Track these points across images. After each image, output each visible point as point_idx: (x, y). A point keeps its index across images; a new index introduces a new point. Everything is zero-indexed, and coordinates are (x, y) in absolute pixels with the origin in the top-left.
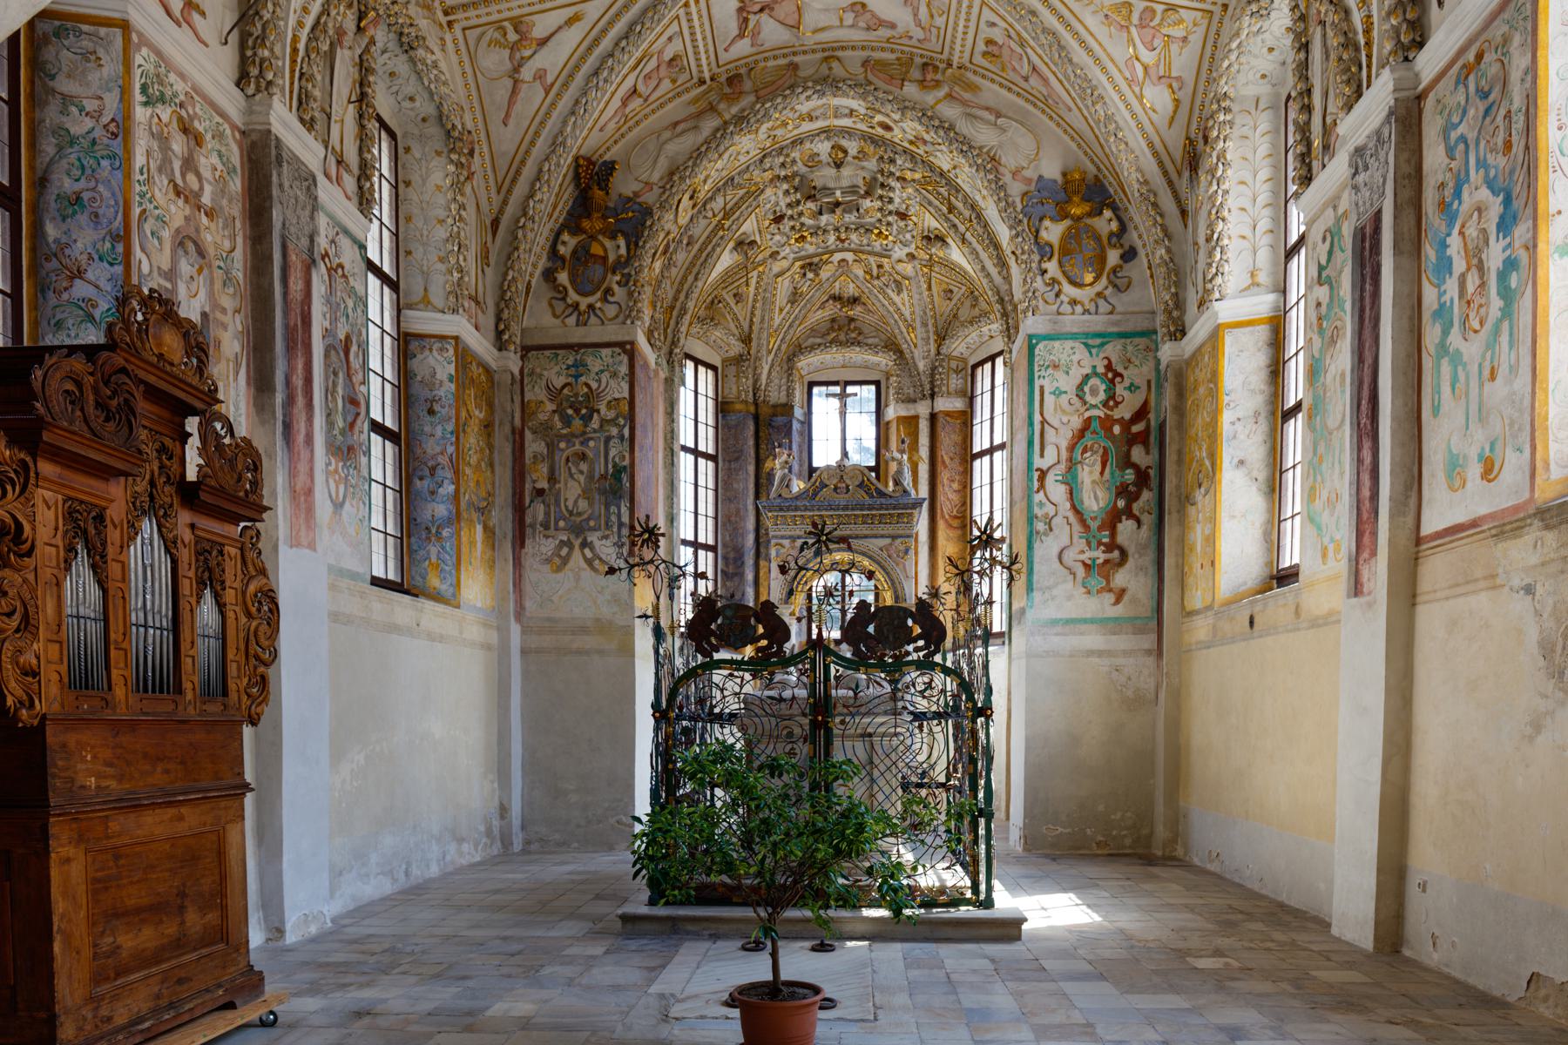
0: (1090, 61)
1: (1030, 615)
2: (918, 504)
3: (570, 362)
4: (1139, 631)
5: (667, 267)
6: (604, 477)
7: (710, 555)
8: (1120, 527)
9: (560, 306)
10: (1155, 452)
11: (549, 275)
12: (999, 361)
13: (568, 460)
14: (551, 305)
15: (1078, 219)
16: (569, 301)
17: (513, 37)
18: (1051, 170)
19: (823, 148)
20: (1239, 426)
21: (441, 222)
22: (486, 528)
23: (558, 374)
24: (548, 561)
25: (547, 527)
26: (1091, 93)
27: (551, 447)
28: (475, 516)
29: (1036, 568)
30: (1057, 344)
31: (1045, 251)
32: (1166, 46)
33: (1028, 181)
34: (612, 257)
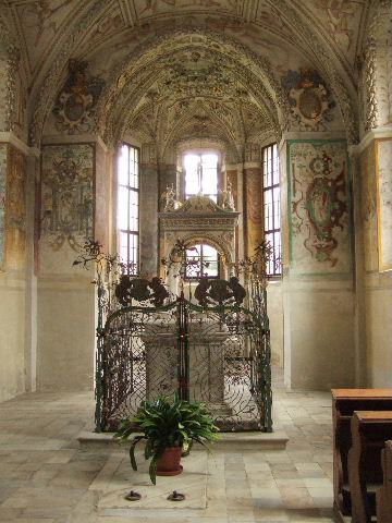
0: (309, 22)
1: (291, 272)
2: (236, 215)
4: (345, 279)
5: (113, 107)
7: (136, 236)
8: (334, 229)
10: (348, 193)
11: (55, 111)
12: (275, 147)
15: (307, 89)
17: (40, 9)
18: (294, 67)
19: (188, 54)
20: (386, 186)
21: (3, 90)
22: (20, 231)
26: (310, 34)
27: (55, 191)
28: (15, 224)
29: (293, 249)
30: (300, 145)
31: (292, 102)
32: (344, 16)
33: (284, 72)
34: (85, 104)
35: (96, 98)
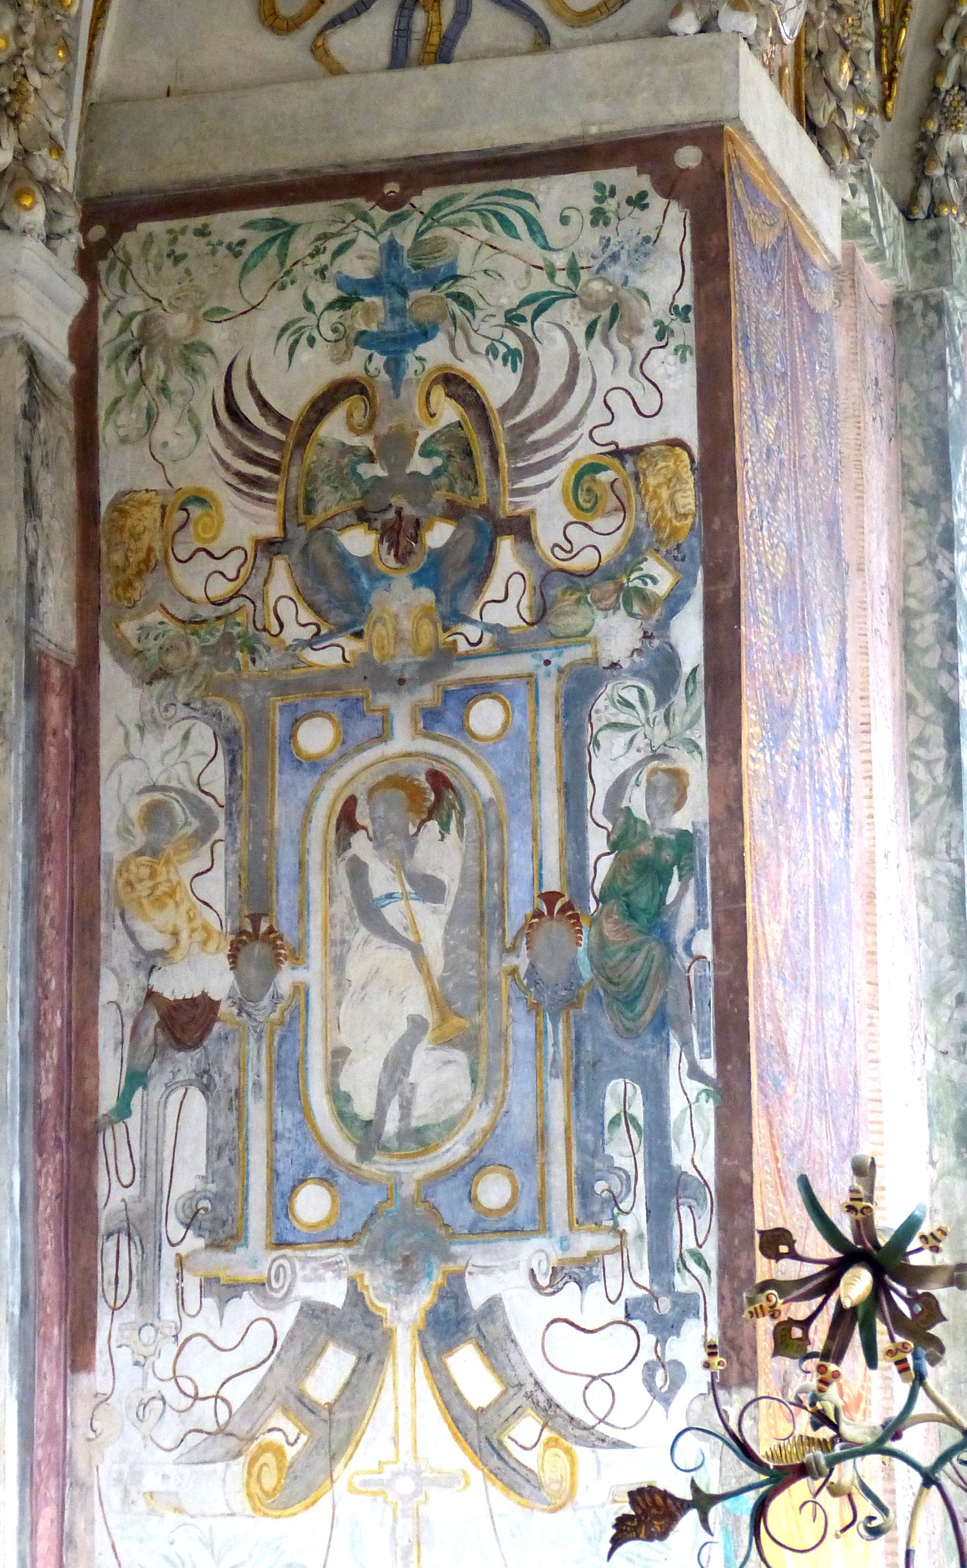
3: (357, 266)
6: (558, 907)
13: (347, 821)
23: (293, 335)
24: (232, 1438)
25: (223, 1231)
27: (251, 752)
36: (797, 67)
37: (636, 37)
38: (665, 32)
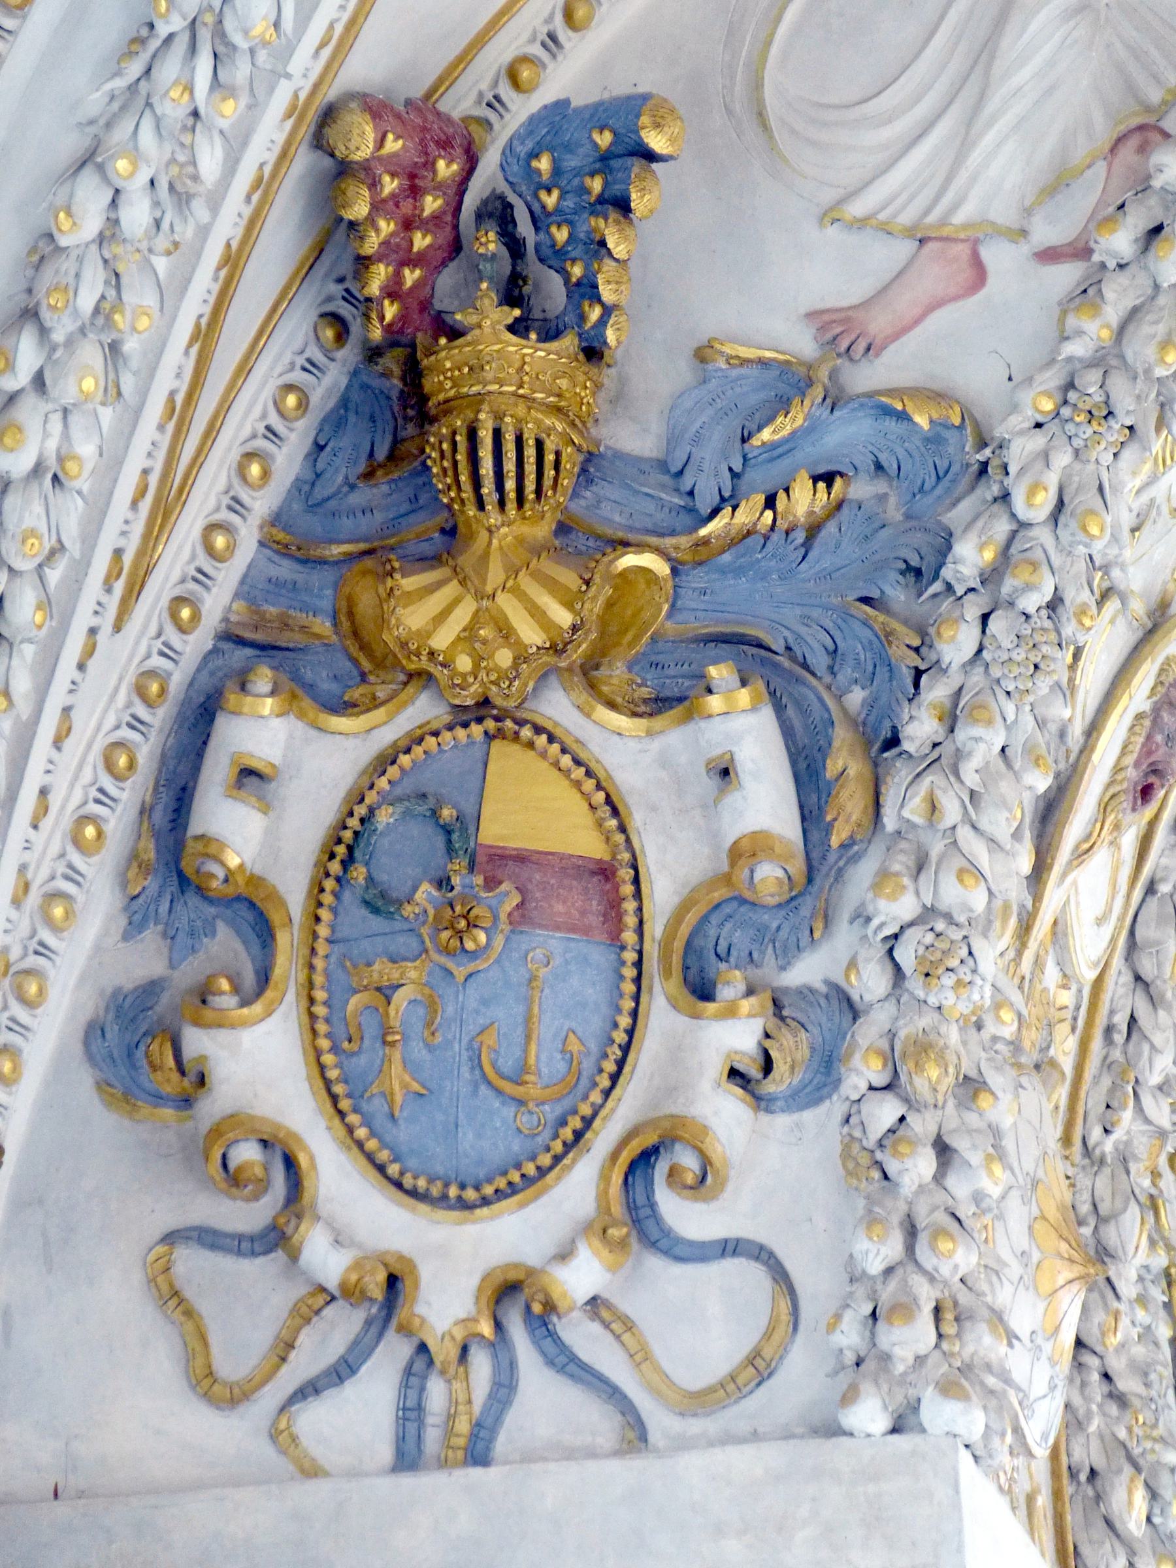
9: (244, 1303)
11: (142, 1051)
14: (173, 1299)
16: (324, 1258)
34: (672, 869)
35: (853, 738)
36: (1057, 1494)
37: (788, 1436)
38: (834, 1430)
